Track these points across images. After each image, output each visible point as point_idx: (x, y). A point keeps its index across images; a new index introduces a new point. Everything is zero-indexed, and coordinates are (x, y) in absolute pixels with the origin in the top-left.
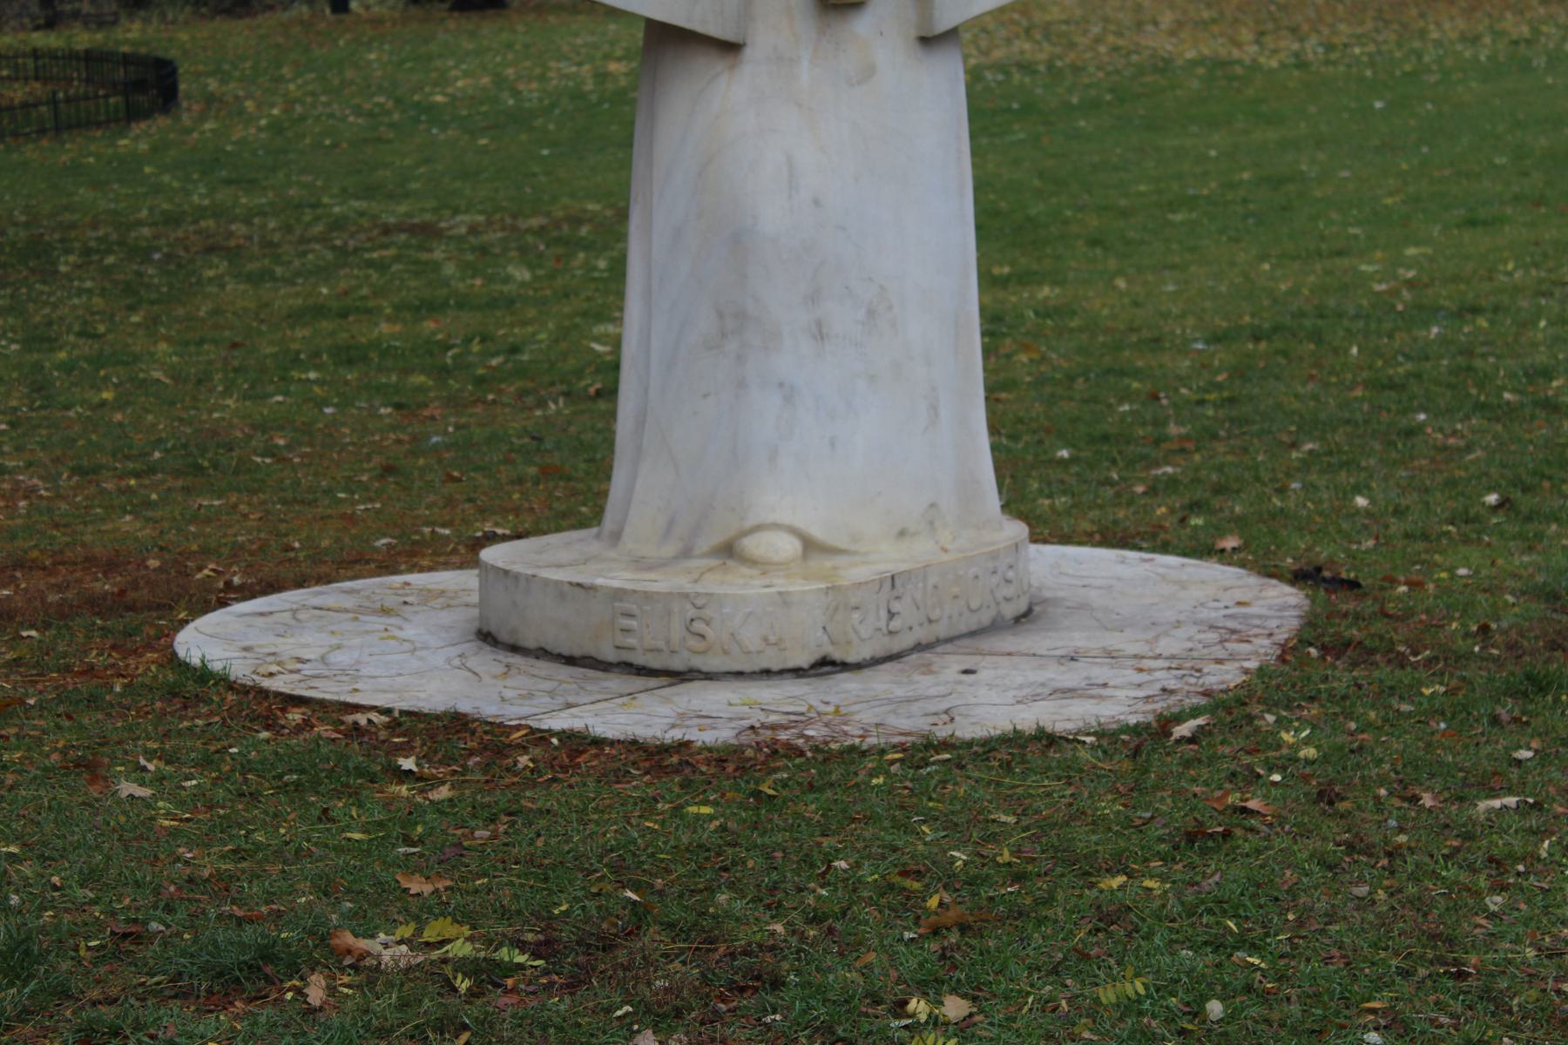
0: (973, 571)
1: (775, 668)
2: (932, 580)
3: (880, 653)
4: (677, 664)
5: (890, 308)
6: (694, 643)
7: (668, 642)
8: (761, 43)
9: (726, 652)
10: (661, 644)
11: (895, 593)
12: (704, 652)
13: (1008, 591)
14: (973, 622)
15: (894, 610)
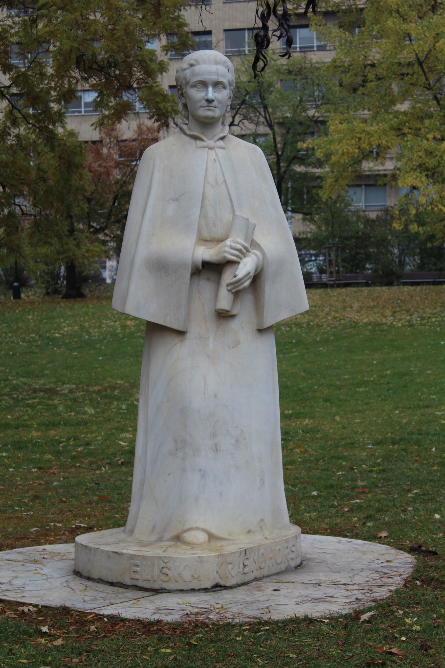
0: (278, 547)
1: (197, 588)
2: (261, 551)
3: (240, 582)
4: (156, 586)
5: (245, 439)
7: (152, 577)
8: (194, 331)
9: (176, 581)
10: (149, 578)
13: (293, 556)
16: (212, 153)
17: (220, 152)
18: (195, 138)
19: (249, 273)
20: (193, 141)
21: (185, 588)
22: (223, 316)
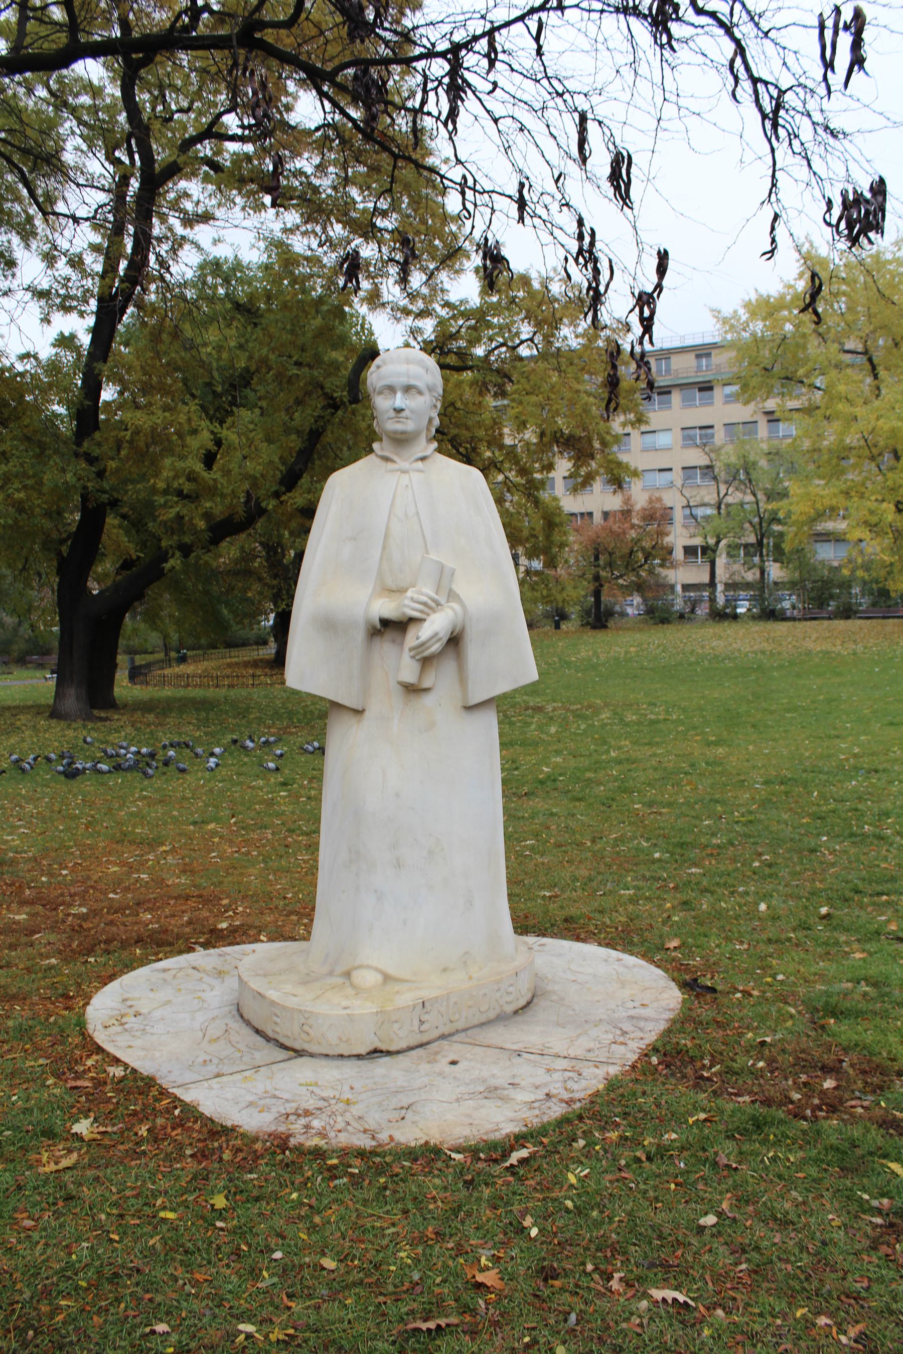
1: (346, 1054)
3: (413, 1043)
4: (297, 1046)
6: (304, 1036)
10: (290, 1034)
12: (309, 1042)
13: (508, 999)
14: (483, 1019)
16: (405, 477)
17: (415, 476)
18: (387, 459)
19: (436, 634)
20: (383, 464)
22: (412, 690)
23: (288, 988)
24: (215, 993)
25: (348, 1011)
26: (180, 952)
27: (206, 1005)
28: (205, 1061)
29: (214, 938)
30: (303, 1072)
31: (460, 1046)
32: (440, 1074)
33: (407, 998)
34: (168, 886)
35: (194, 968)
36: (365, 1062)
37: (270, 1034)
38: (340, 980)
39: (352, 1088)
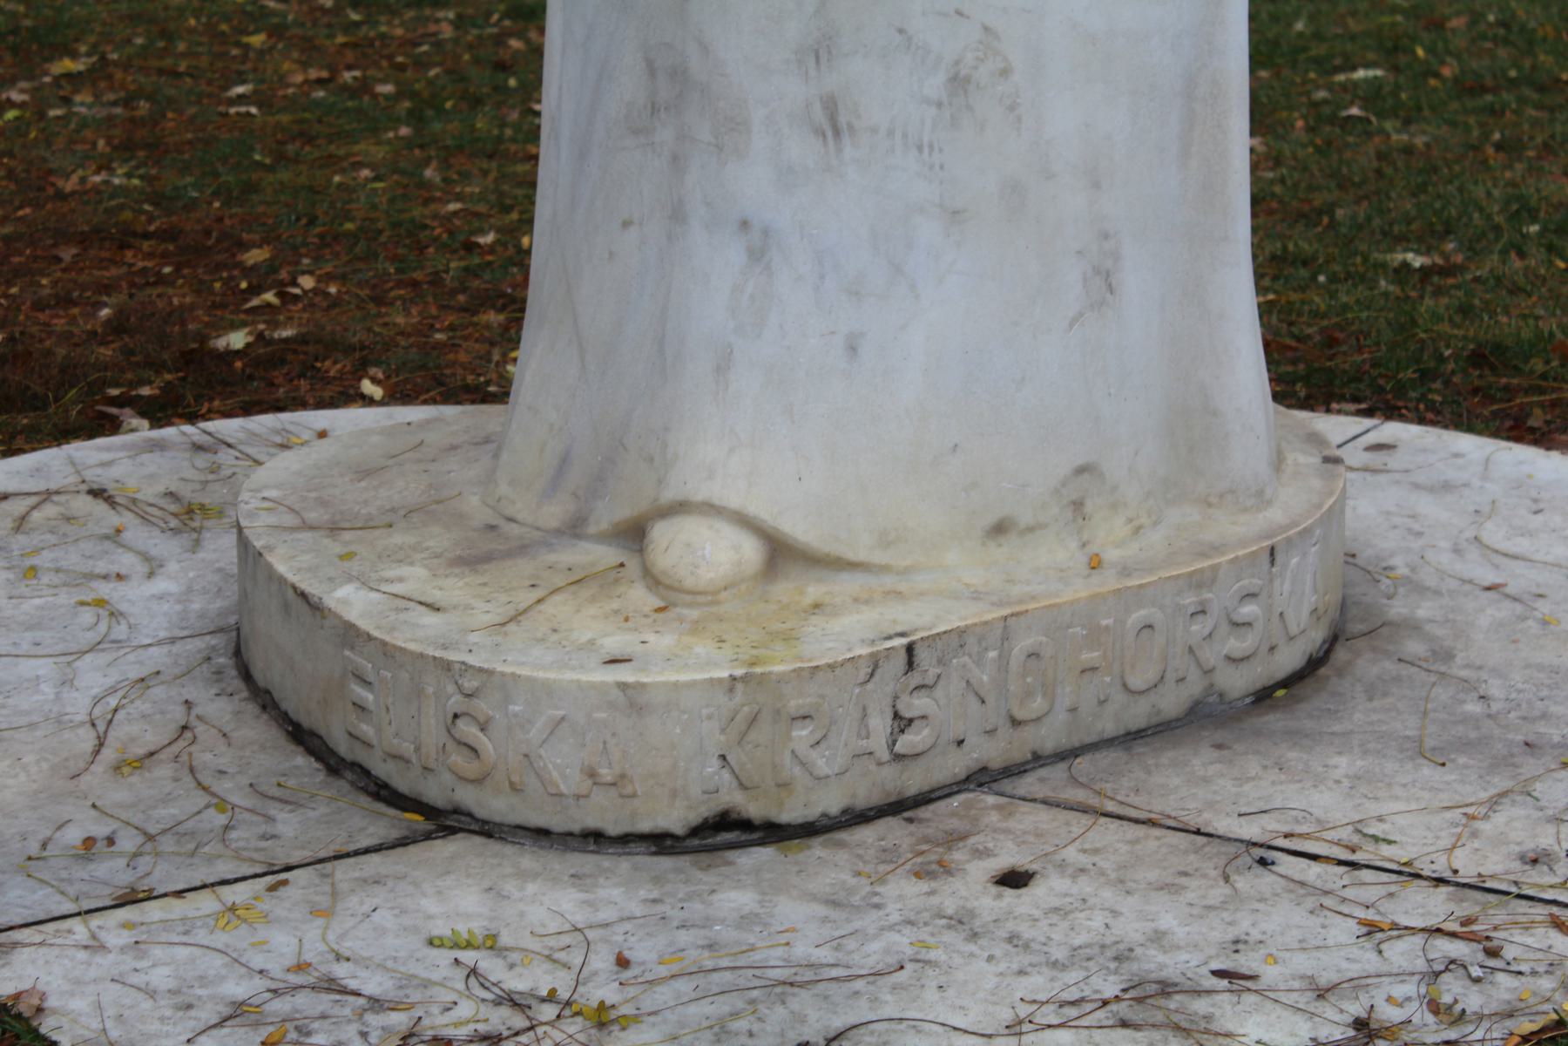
0: (1137, 616)
1: (613, 830)
4: (434, 792)
5: (1005, 72)
6: (458, 759)
7: (418, 749)
9: (515, 788)
10: (407, 749)
11: (915, 679)
12: (478, 781)
13: (1237, 645)
14: (1138, 714)
15: (907, 714)
21: (557, 823)
23: (414, 578)
24: (161, 585)
25: (624, 674)
26: (64, 434)
27: (120, 631)
28: (89, 842)
29: (196, 386)
30: (452, 892)
31: (1043, 817)
32: (960, 921)
33: (847, 628)
34: (61, 196)
35: (97, 493)
36: (684, 861)
37: (343, 747)
38: (605, 555)
39: (623, 962)
